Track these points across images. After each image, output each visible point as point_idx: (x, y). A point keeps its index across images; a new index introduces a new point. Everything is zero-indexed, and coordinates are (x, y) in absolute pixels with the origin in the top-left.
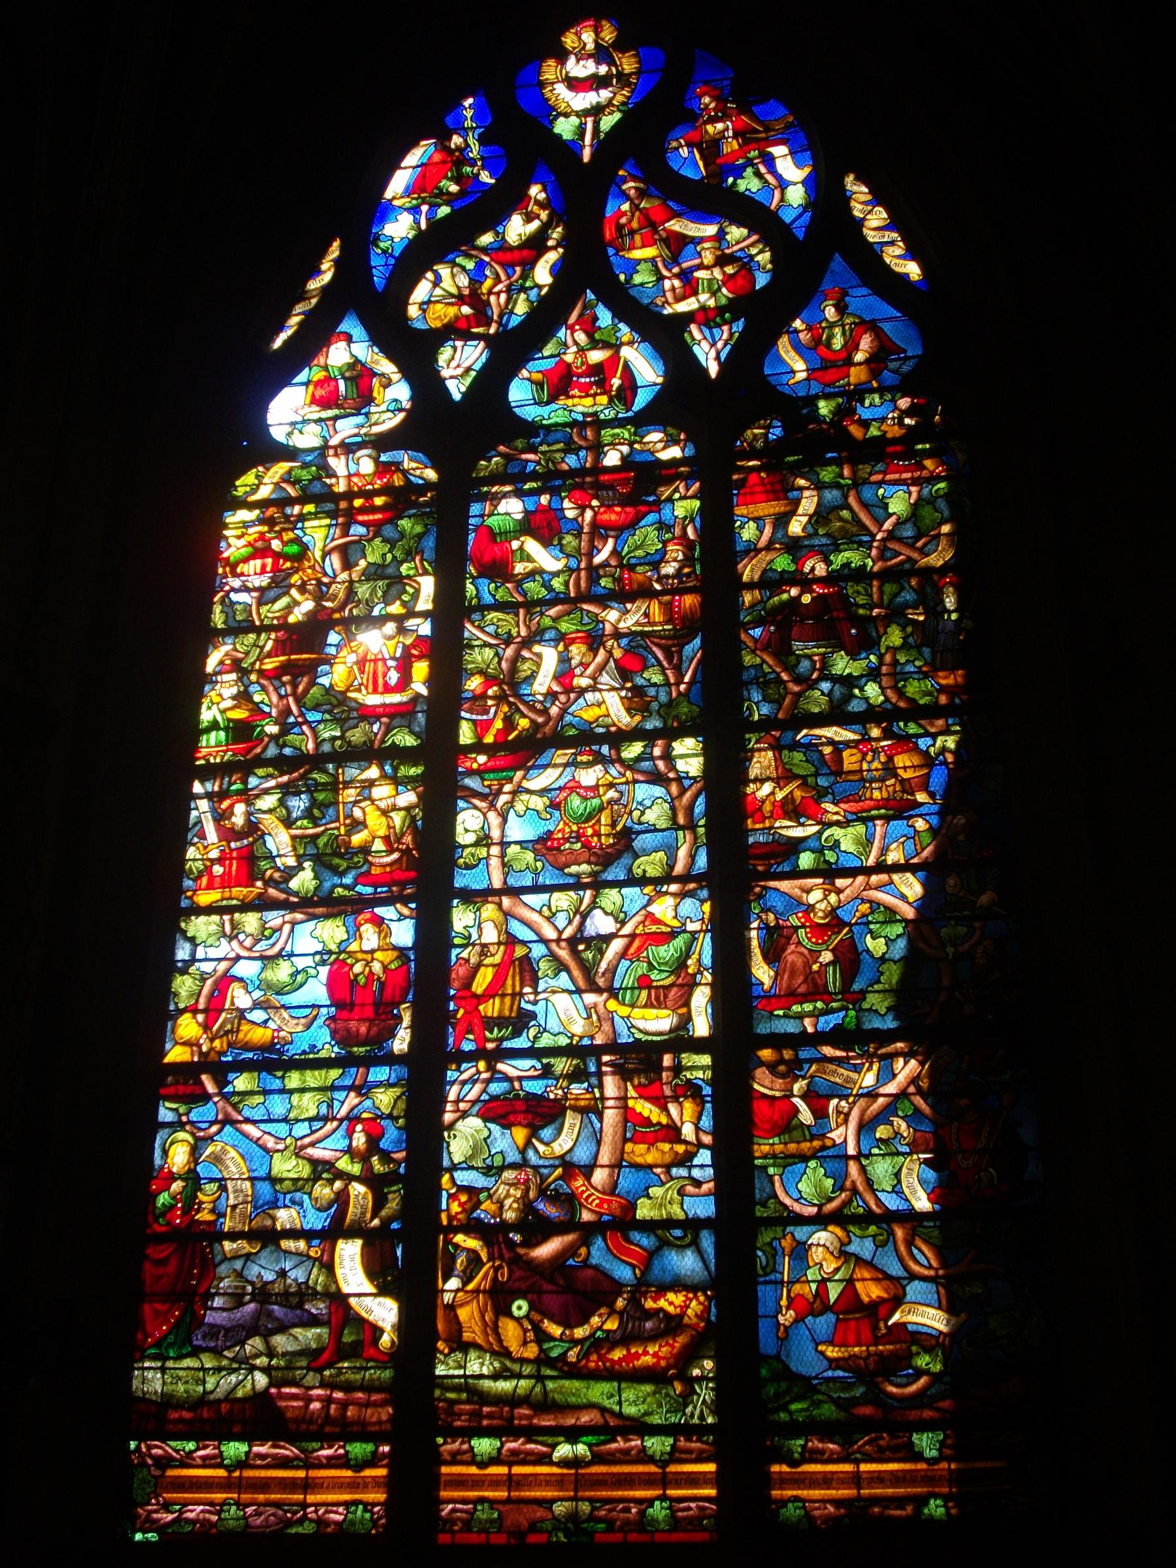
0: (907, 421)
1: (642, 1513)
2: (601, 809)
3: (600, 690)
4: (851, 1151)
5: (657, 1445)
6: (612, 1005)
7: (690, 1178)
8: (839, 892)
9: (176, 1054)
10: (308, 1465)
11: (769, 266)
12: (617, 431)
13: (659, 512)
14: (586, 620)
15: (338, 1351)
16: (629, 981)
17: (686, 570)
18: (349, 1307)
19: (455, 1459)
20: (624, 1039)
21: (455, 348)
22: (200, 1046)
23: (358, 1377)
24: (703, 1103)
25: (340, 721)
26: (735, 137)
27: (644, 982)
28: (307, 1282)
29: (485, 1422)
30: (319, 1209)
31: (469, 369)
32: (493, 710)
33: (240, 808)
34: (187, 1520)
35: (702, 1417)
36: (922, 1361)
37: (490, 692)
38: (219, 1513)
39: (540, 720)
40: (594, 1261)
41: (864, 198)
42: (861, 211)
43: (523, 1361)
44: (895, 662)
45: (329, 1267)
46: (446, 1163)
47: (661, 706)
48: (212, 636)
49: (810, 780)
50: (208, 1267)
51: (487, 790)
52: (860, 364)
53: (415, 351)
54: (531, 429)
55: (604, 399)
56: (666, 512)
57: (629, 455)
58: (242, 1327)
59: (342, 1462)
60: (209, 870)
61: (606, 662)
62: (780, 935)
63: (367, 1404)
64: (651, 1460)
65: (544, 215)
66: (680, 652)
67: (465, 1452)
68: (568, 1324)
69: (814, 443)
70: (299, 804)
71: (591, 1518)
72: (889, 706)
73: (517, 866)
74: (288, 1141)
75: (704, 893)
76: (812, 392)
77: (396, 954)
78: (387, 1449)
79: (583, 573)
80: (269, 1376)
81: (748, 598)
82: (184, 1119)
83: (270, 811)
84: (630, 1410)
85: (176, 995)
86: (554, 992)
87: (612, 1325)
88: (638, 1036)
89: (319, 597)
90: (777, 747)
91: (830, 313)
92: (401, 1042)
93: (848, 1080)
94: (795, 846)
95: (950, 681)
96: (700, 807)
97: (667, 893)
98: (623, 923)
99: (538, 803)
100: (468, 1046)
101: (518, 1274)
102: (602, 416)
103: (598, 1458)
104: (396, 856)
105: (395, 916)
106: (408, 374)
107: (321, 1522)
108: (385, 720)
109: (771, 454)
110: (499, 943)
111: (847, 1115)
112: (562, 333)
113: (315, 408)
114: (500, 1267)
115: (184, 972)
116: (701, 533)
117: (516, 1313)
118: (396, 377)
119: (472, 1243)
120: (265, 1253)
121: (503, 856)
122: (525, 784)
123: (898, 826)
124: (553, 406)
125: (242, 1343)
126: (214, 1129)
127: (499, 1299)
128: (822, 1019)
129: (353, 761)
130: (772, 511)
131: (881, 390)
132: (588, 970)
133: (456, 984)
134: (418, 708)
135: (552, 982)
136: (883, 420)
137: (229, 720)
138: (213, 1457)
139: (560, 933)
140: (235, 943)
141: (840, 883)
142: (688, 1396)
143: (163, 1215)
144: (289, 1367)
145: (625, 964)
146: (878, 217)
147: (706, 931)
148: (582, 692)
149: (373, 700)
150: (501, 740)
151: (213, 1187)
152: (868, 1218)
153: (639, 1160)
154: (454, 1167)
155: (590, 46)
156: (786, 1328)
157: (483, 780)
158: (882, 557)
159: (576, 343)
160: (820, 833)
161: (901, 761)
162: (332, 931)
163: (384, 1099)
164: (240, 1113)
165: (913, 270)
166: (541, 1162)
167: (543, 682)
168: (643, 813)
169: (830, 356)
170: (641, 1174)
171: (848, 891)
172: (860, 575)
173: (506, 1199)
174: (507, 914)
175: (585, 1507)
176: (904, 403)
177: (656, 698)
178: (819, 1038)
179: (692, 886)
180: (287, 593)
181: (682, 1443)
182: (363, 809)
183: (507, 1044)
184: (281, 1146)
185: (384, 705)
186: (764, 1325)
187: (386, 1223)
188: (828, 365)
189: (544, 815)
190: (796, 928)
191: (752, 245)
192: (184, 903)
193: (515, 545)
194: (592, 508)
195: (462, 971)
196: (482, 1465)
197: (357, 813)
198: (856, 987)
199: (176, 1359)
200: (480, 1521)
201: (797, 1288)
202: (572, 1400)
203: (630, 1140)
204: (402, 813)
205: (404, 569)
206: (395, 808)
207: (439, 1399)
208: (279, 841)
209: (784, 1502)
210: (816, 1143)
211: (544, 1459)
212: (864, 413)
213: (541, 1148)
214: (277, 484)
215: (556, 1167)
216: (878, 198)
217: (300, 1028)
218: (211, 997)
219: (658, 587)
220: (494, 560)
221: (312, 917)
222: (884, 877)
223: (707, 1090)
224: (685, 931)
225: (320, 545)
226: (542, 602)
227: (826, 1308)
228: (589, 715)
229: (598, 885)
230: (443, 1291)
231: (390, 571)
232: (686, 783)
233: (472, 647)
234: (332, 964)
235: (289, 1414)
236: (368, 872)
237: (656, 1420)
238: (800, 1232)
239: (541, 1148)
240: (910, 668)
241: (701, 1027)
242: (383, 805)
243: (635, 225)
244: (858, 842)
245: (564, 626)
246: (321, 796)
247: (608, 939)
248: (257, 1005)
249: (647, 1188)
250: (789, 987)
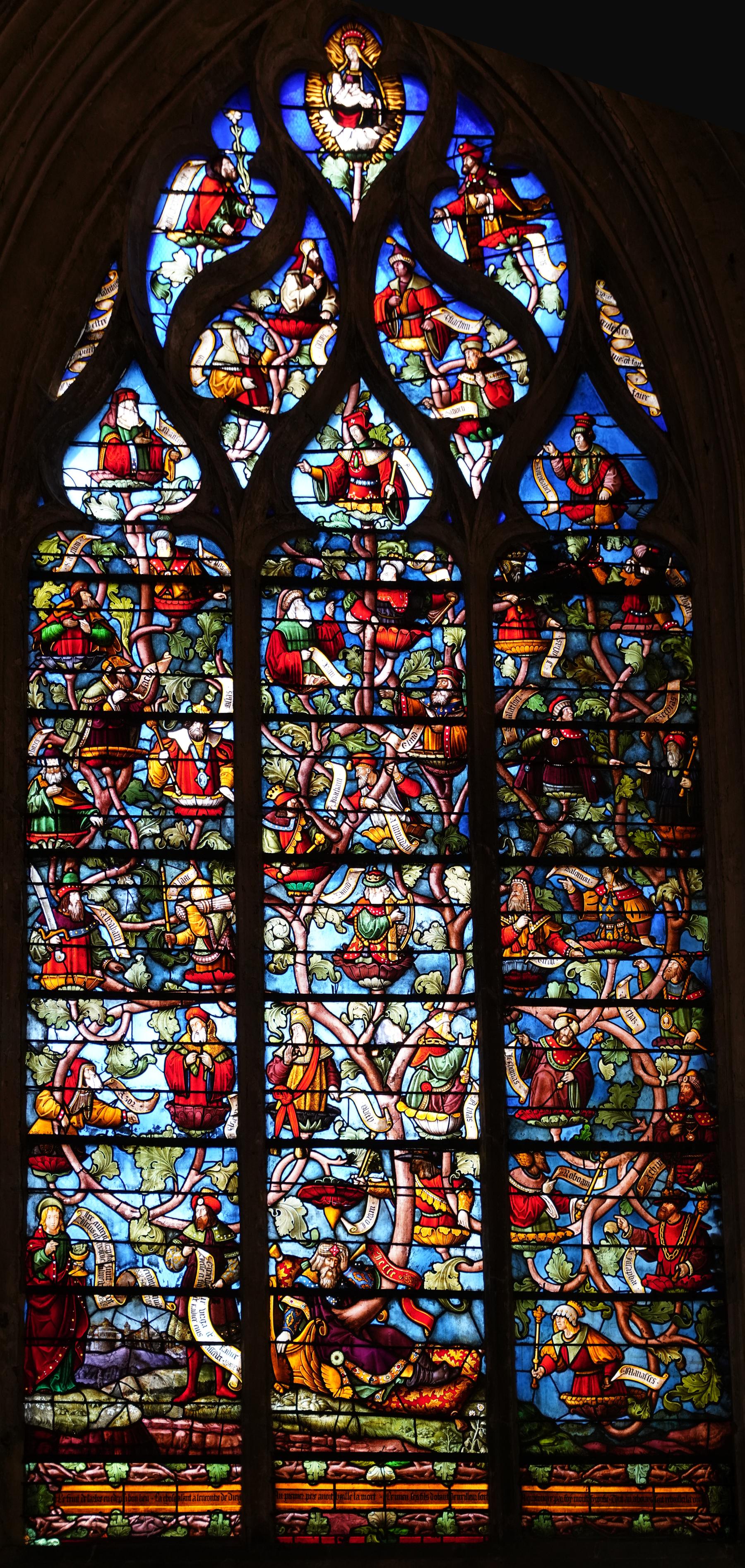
0: (643, 570)
1: (434, 1521)
2: (388, 928)
3: (384, 813)
4: (586, 1242)
5: (444, 1469)
6: (401, 1106)
7: (464, 1257)
8: (579, 1020)
9: (40, 1128)
10: (178, 1482)
11: (526, 379)
12: (392, 544)
13: (430, 636)
14: (370, 741)
15: (196, 1390)
16: (414, 1088)
17: (455, 701)
18: (204, 1354)
19: (292, 1478)
20: (411, 1137)
21: (238, 426)
22: (59, 1121)
23: (214, 1411)
24: (474, 1195)
25: (159, 819)
26: (495, 215)
27: (426, 1090)
28: (166, 1332)
29: (314, 1449)
30: (172, 1270)
31: (253, 453)
32: (292, 822)
34: (83, 1527)
35: (476, 1448)
36: (635, 1410)
37: (289, 804)
38: (108, 1521)
39: (334, 836)
40: (392, 1322)
41: (612, 311)
42: (610, 327)
43: (341, 1400)
44: (627, 813)
45: (184, 1320)
46: (272, 1235)
47: (435, 834)
48: (33, 716)
49: (557, 916)
50: (84, 1317)
51: (291, 901)
52: (603, 502)
53: (202, 423)
54: (316, 528)
55: (378, 507)
56: (437, 637)
57: (404, 572)
58: (117, 1368)
59: (205, 1479)
60: (50, 955)
61: (389, 786)
62: (533, 1055)
63: (222, 1433)
64: (439, 1480)
65: (317, 280)
66: (450, 782)
67: (300, 1472)
68: (374, 1372)
69: (563, 581)
70: (127, 899)
71: (397, 1524)
72: (620, 854)
73: (319, 976)
74: (143, 1210)
75: (473, 1013)
76: (563, 526)
77: (221, 1048)
78: (239, 1469)
79: (366, 692)
80: (141, 1409)
81: (508, 734)
82: (52, 1186)
83: (101, 903)
84: (423, 1441)
85: (34, 1072)
86: (354, 1092)
87: (407, 1374)
88: (423, 1135)
89: (129, 688)
90: (531, 882)
91: (580, 440)
92: (230, 1128)
93: (584, 1183)
94: (545, 976)
95: (670, 835)
96: (468, 933)
97: (442, 1010)
98: (408, 1035)
99: (334, 916)
100: (286, 1135)
101: (334, 1330)
102: (378, 527)
103: (401, 1478)
104: (215, 956)
105: (220, 1013)
106: (197, 451)
107: (190, 1527)
108: (198, 822)
109: (526, 588)
110: (307, 1045)
111: (583, 1212)
112: (337, 424)
113: (108, 475)
114: (320, 1324)
115: (39, 1052)
116: (467, 663)
117: (334, 1362)
118: (185, 451)
119: (298, 1304)
120: (130, 1306)
121: (307, 964)
122: (324, 898)
123: (626, 967)
124: (333, 508)
125: (117, 1382)
126: (79, 1196)
127: (321, 1351)
128: (565, 1130)
129: (173, 859)
130: (527, 649)
131: (621, 533)
132: (381, 1074)
133: (274, 1079)
134: (227, 814)
135: (353, 1083)
136: (622, 565)
137: (57, 807)
138: (101, 1475)
139: (358, 1039)
140: (81, 1028)
141: (580, 1012)
142: (466, 1431)
143: (41, 1270)
144: (157, 1402)
145: (410, 1071)
146: (623, 339)
147: (474, 1047)
148: (369, 812)
149: (187, 800)
150: (300, 851)
151: (81, 1248)
152: (598, 1297)
153: (425, 1240)
154: (280, 1240)
155: (355, 66)
156: (538, 1380)
157: (288, 890)
158: (617, 708)
159: (352, 440)
160: (564, 966)
161: (630, 906)
162: (168, 1024)
163: (221, 1178)
164: (99, 1183)
165: (652, 402)
166: (349, 1238)
167: (334, 800)
168: (422, 934)
169: (578, 490)
170: (427, 1252)
171: (585, 1021)
172: (598, 723)
173: (323, 1268)
174: (312, 1018)
175: (392, 1516)
176: (640, 550)
177: (431, 826)
178: (563, 1146)
179: (462, 1005)
180: (99, 679)
181: (462, 1468)
182: (185, 909)
183: (317, 1136)
184: (137, 1215)
185: (196, 807)
186: (522, 1381)
187: (227, 1284)
188: (578, 501)
189: (340, 929)
190: (545, 1050)
191: (510, 351)
192: (34, 986)
193: (305, 655)
194: (372, 625)
195: (278, 1067)
196: (313, 1483)
197: (180, 912)
198: (591, 1104)
199: (63, 1394)
200: (314, 1526)
201: (545, 1350)
202: (379, 1432)
203: (418, 1224)
204: (219, 916)
205: (206, 666)
206: (212, 911)
207: (278, 1430)
208: (111, 932)
209: (537, 1514)
210: (560, 1234)
211: (360, 1478)
212: (608, 557)
213: (349, 1226)
214: (79, 557)
215: (361, 1243)
216: (627, 315)
217: (145, 1110)
218: (65, 1077)
219: (431, 715)
220: (287, 669)
221: (150, 1008)
222: (613, 1010)
223: (477, 1185)
224: (458, 1046)
225: (126, 631)
226: (330, 718)
227: (566, 1366)
228: (376, 835)
229: (387, 999)
230: (276, 1342)
231: (193, 667)
232: (458, 909)
233: (271, 757)
234: (168, 1054)
235: (159, 1441)
236: (194, 969)
237: (442, 1449)
238: (548, 1305)
239: (349, 1226)
240: (638, 820)
241: (471, 1131)
242: (201, 905)
243: (403, 308)
244: (594, 977)
245: (351, 745)
246: (147, 893)
247: (396, 1047)
248: (105, 1087)
249: (432, 1264)
250: (539, 1100)
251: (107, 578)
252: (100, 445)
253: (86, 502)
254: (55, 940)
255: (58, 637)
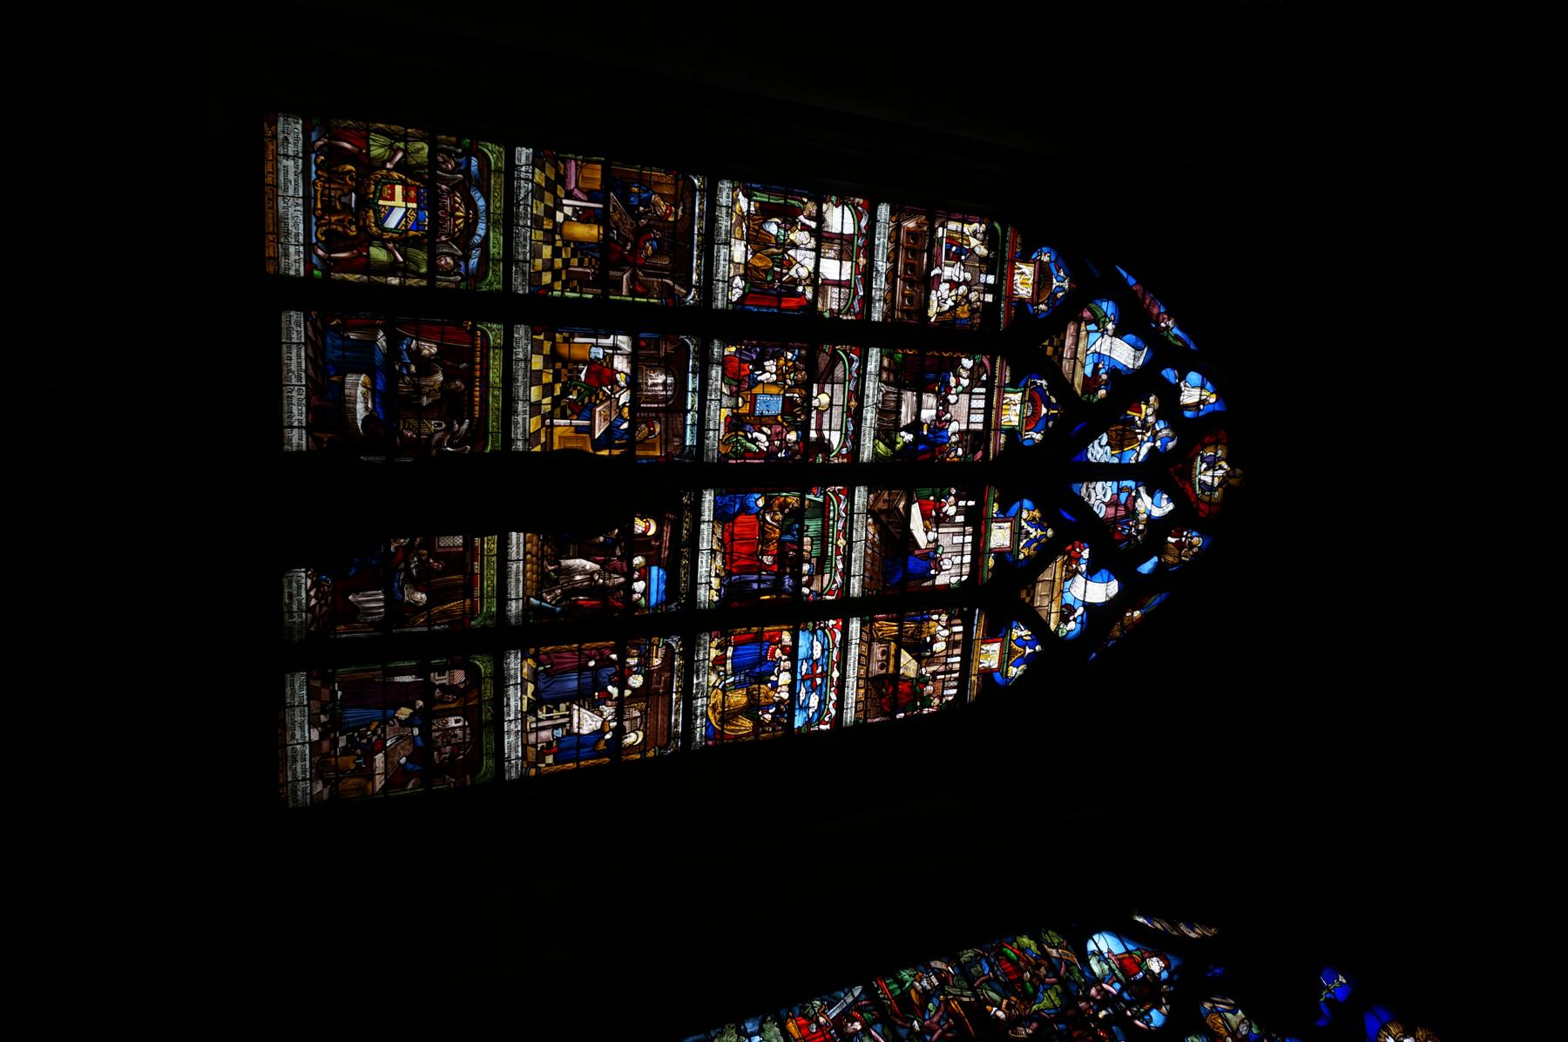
33: (858, 1026)
48: (953, 959)
192: (783, 1013)
251: (1061, 981)
252: (1128, 952)
253: (1093, 953)
254: (822, 1020)
255: (1009, 959)
